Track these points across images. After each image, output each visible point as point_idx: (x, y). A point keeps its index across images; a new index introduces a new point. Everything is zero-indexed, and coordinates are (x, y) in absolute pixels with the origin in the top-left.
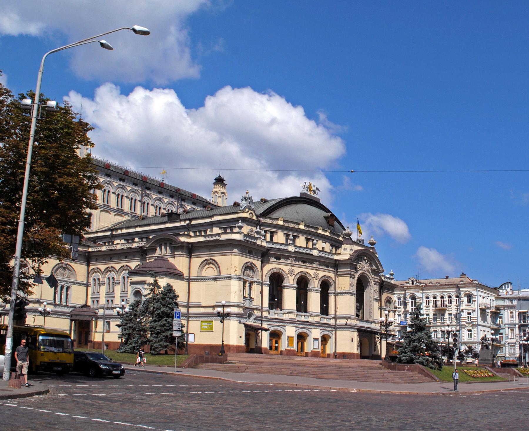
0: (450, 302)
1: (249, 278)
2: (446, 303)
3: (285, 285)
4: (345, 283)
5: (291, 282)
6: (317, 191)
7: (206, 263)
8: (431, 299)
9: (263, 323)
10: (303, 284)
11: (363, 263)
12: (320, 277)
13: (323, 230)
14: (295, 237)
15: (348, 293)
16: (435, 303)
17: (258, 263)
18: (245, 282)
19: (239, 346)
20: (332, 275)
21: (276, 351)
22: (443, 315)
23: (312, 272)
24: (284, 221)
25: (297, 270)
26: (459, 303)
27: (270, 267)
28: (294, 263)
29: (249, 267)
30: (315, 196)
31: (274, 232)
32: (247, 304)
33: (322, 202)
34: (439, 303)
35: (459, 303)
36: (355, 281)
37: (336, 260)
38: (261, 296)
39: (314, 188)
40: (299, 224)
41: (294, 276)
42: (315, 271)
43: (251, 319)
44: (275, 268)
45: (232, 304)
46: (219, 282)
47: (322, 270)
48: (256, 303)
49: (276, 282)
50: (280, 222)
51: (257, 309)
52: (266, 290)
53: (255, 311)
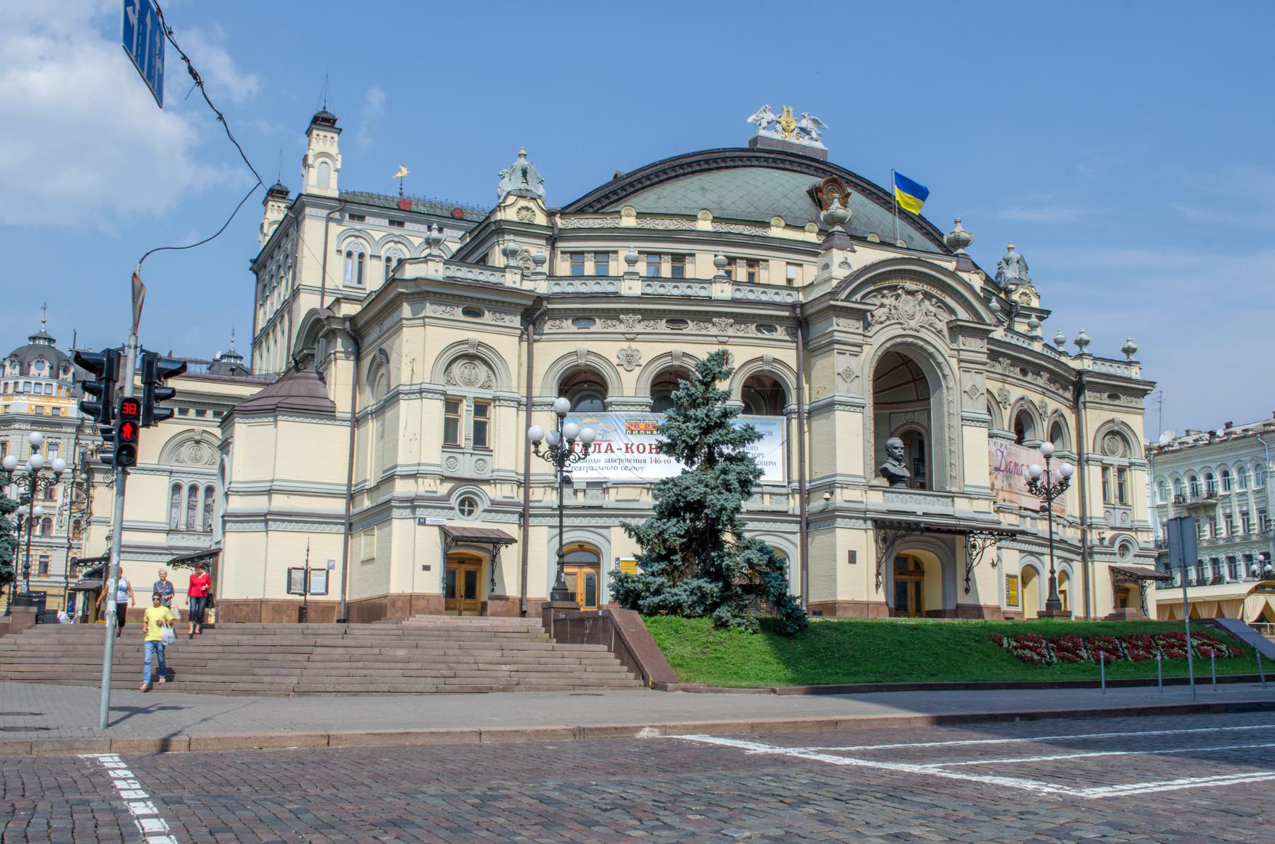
9: (566, 521)
11: (907, 304)
14: (678, 258)
18: (452, 405)
24: (640, 215)
27: (557, 349)
28: (639, 328)
30: (805, 141)
31: (607, 253)
32: (466, 466)
37: (793, 306)
40: (693, 218)
41: (638, 370)
47: (745, 341)
50: (629, 221)
53: (486, 488)
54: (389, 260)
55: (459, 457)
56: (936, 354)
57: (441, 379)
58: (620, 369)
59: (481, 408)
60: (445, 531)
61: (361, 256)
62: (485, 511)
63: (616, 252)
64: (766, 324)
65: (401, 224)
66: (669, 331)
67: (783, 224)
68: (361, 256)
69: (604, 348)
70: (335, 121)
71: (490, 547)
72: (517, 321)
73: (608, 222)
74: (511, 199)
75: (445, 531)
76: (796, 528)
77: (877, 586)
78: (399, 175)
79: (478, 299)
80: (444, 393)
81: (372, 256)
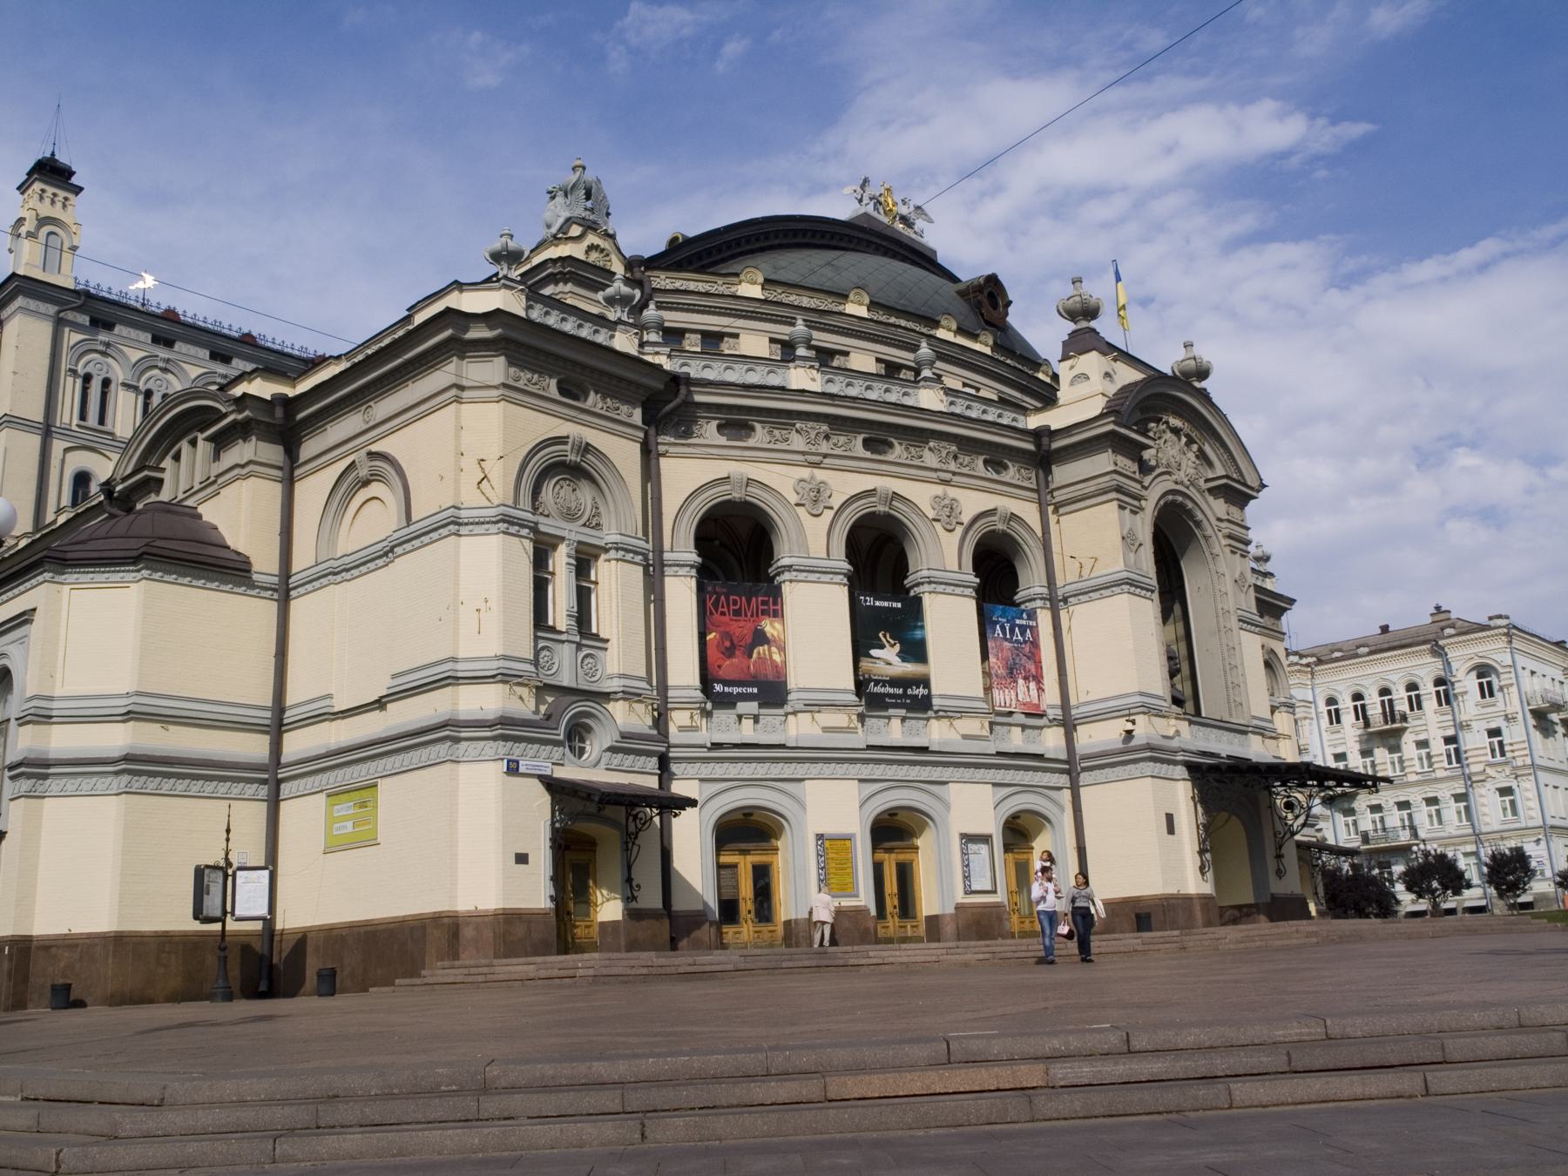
0: (1416, 703)
1: (576, 526)
2: (1402, 706)
3: (785, 562)
4: (1094, 538)
5: (817, 546)
6: (920, 224)
7: (351, 484)
8: (1346, 704)
10: (877, 557)
12: (966, 518)
13: (960, 331)
15: (1117, 583)
16: (1361, 713)
17: (623, 453)
19: (509, 918)
20: (1029, 512)
21: (765, 928)
22: (1395, 749)
23: (922, 494)
24: (768, 283)
25: (844, 484)
26: (1446, 697)
27: (693, 473)
28: (825, 447)
29: (563, 467)
33: (941, 260)
34: (1375, 711)
35: (1446, 697)
36: (1144, 528)
37: (1040, 434)
38: (647, 626)
39: (904, 210)
41: (829, 515)
42: (939, 490)
43: (595, 746)
44: (726, 480)
45: (462, 668)
46: (404, 565)
48: (620, 659)
49: (737, 551)
50: (751, 289)
51: (629, 696)
52: (681, 593)
54: (148, 394)
55: (557, 647)
56: (1205, 522)
57: (525, 501)
58: (800, 510)
59: (583, 563)
60: (551, 784)
61: (106, 383)
62: (613, 750)
63: (736, 336)
64: (997, 457)
65: (169, 344)
66: (868, 455)
67: (954, 327)
68: (106, 383)
69: (774, 476)
70: (72, 173)
71: (620, 813)
72: (637, 416)
73: (719, 286)
74: (575, 231)
75: (551, 784)
76: (1063, 780)
77: (1202, 868)
78: (141, 285)
79: (584, 367)
80: (534, 529)
81: (124, 384)
